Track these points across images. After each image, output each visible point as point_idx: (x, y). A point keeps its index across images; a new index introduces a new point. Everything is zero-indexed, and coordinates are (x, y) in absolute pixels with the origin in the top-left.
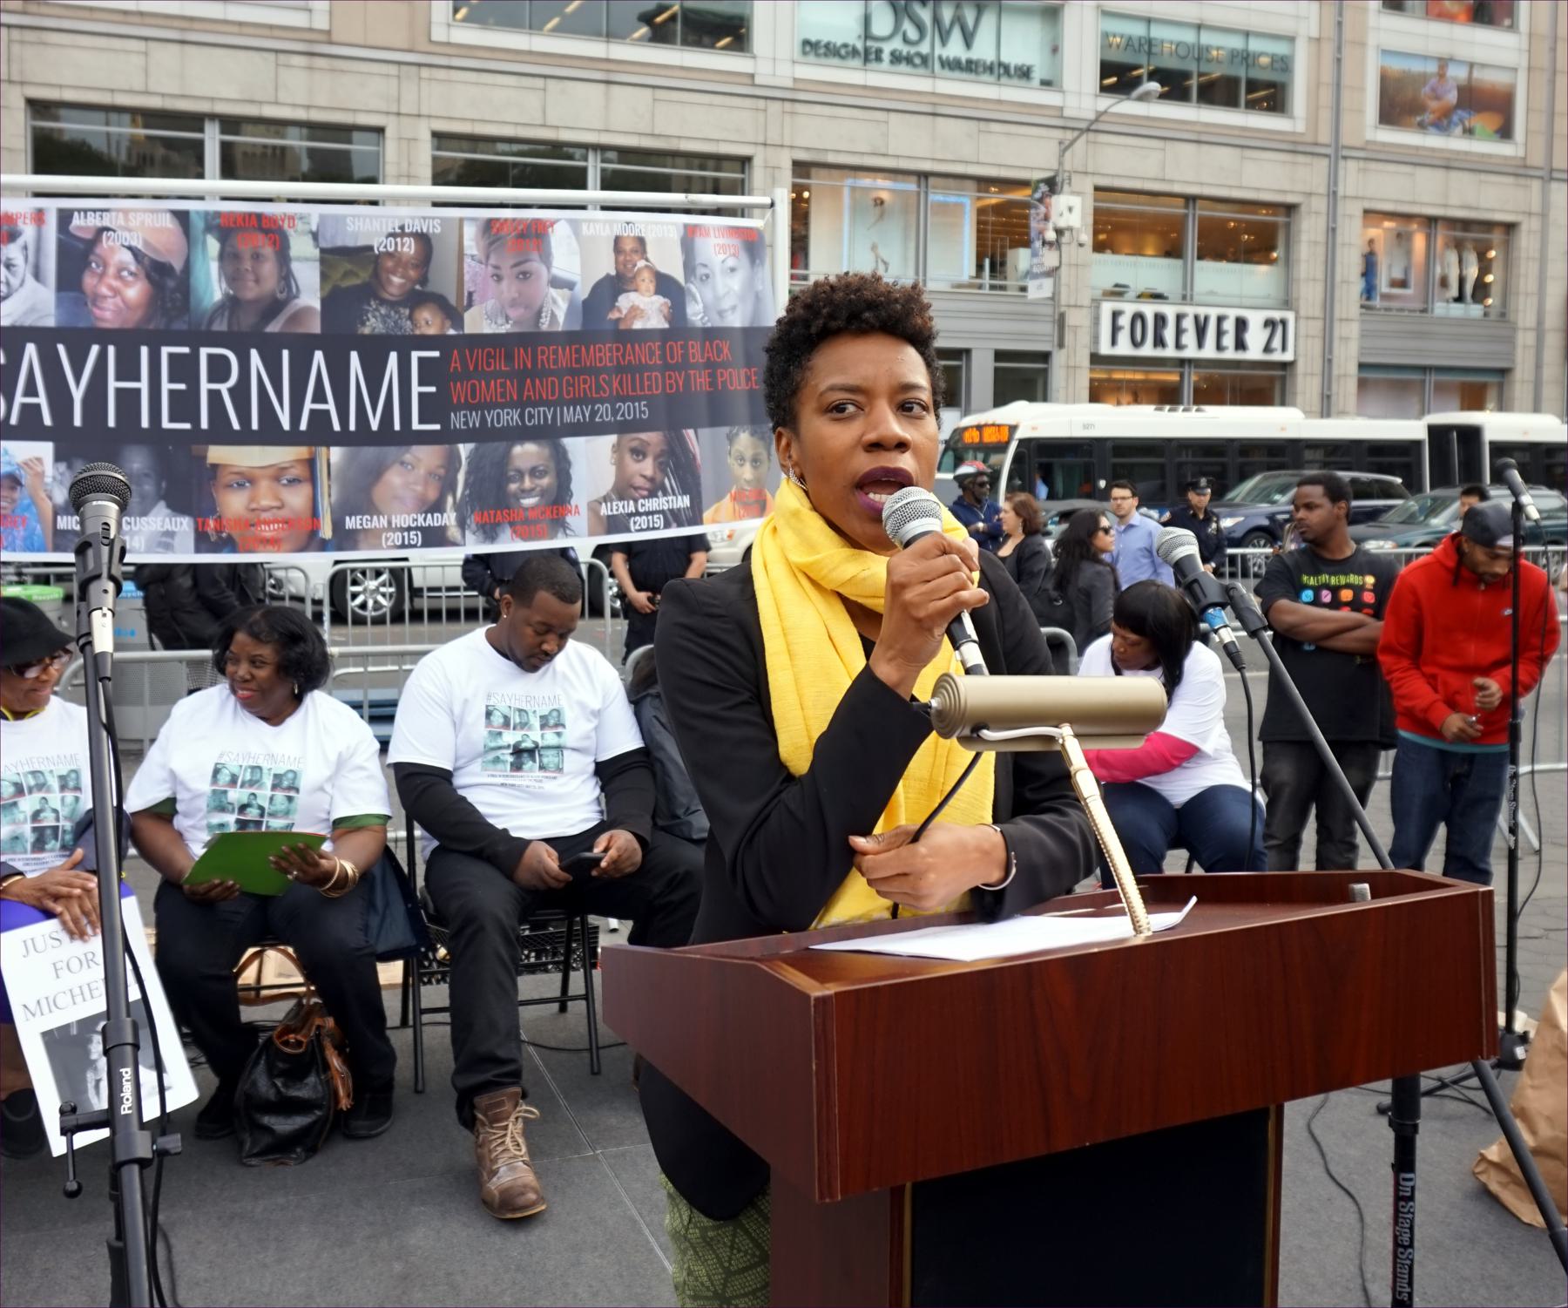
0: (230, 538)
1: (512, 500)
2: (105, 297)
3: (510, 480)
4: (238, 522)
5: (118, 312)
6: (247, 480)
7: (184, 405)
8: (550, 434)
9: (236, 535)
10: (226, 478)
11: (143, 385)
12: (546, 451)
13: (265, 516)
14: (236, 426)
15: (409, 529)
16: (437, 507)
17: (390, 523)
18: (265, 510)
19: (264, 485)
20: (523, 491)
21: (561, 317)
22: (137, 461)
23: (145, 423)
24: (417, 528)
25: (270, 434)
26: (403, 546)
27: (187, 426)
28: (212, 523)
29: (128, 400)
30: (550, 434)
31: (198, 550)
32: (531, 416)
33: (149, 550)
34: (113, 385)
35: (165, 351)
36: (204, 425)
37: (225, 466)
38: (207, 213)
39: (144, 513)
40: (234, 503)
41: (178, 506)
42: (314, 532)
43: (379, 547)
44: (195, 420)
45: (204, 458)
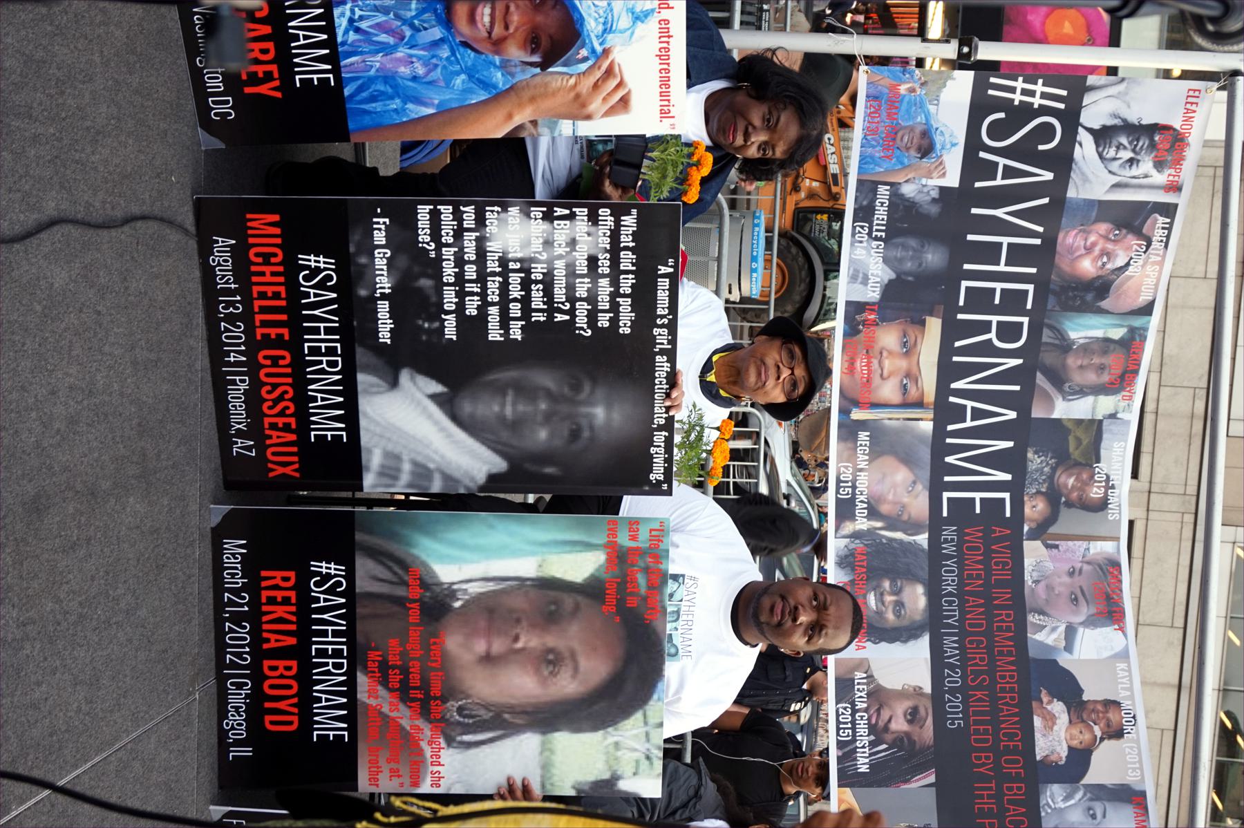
0: (859, 332)
1: (874, 583)
2: (1086, 240)
3: (893, 581)
4: (871, 342)
5: (1071, 250)
6: (909, 349)
7: (980, 300)
8: (934, 624)
9: (861, 337)
10: (912, 332)
11: (1002, 268)
12: (918, 617)
13: (875, 362)
14: (957, 344)
15: (854, 487)
16: (873, 513)
17: (861, 470)
18: (880, 363)
19: (903, 364)
20: (882, 594)
21: (1040, 637)
22: (934, 257)
23: (966, 267)
24: (854, 494)
25: (948, 371)
26: (839, 481)
27: (961, 303)
28: (872, 317)
29: (991, 254)
30: (934, 624)
31: (848, 303)
32: (950, 603)
33: (851, 261)
34: (1005, 240)
35: (1030, 288)
36: (960, 316)
37: (923, 333)
38: (1146, 329)
39: (885, 261)
40: (889, 338)
41: (891, 290)
42: (857, 404)
43: (840, 460)
44: (964, 310)
45: (931, 315)
